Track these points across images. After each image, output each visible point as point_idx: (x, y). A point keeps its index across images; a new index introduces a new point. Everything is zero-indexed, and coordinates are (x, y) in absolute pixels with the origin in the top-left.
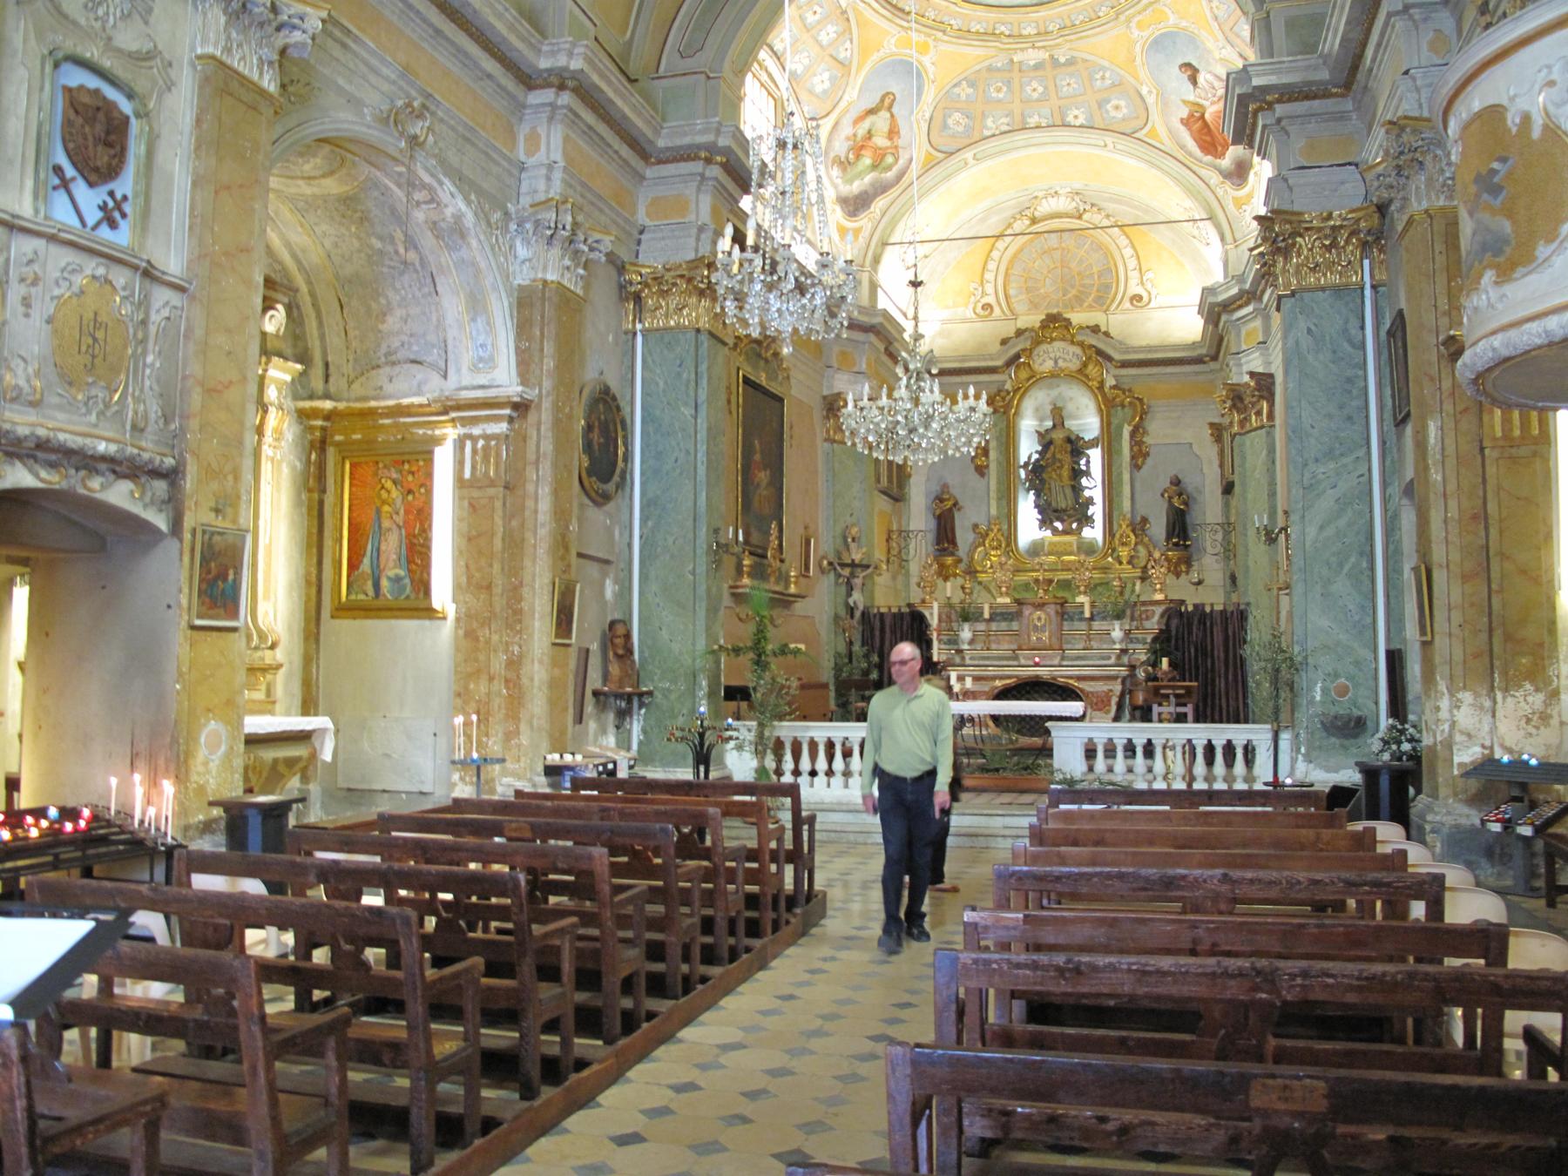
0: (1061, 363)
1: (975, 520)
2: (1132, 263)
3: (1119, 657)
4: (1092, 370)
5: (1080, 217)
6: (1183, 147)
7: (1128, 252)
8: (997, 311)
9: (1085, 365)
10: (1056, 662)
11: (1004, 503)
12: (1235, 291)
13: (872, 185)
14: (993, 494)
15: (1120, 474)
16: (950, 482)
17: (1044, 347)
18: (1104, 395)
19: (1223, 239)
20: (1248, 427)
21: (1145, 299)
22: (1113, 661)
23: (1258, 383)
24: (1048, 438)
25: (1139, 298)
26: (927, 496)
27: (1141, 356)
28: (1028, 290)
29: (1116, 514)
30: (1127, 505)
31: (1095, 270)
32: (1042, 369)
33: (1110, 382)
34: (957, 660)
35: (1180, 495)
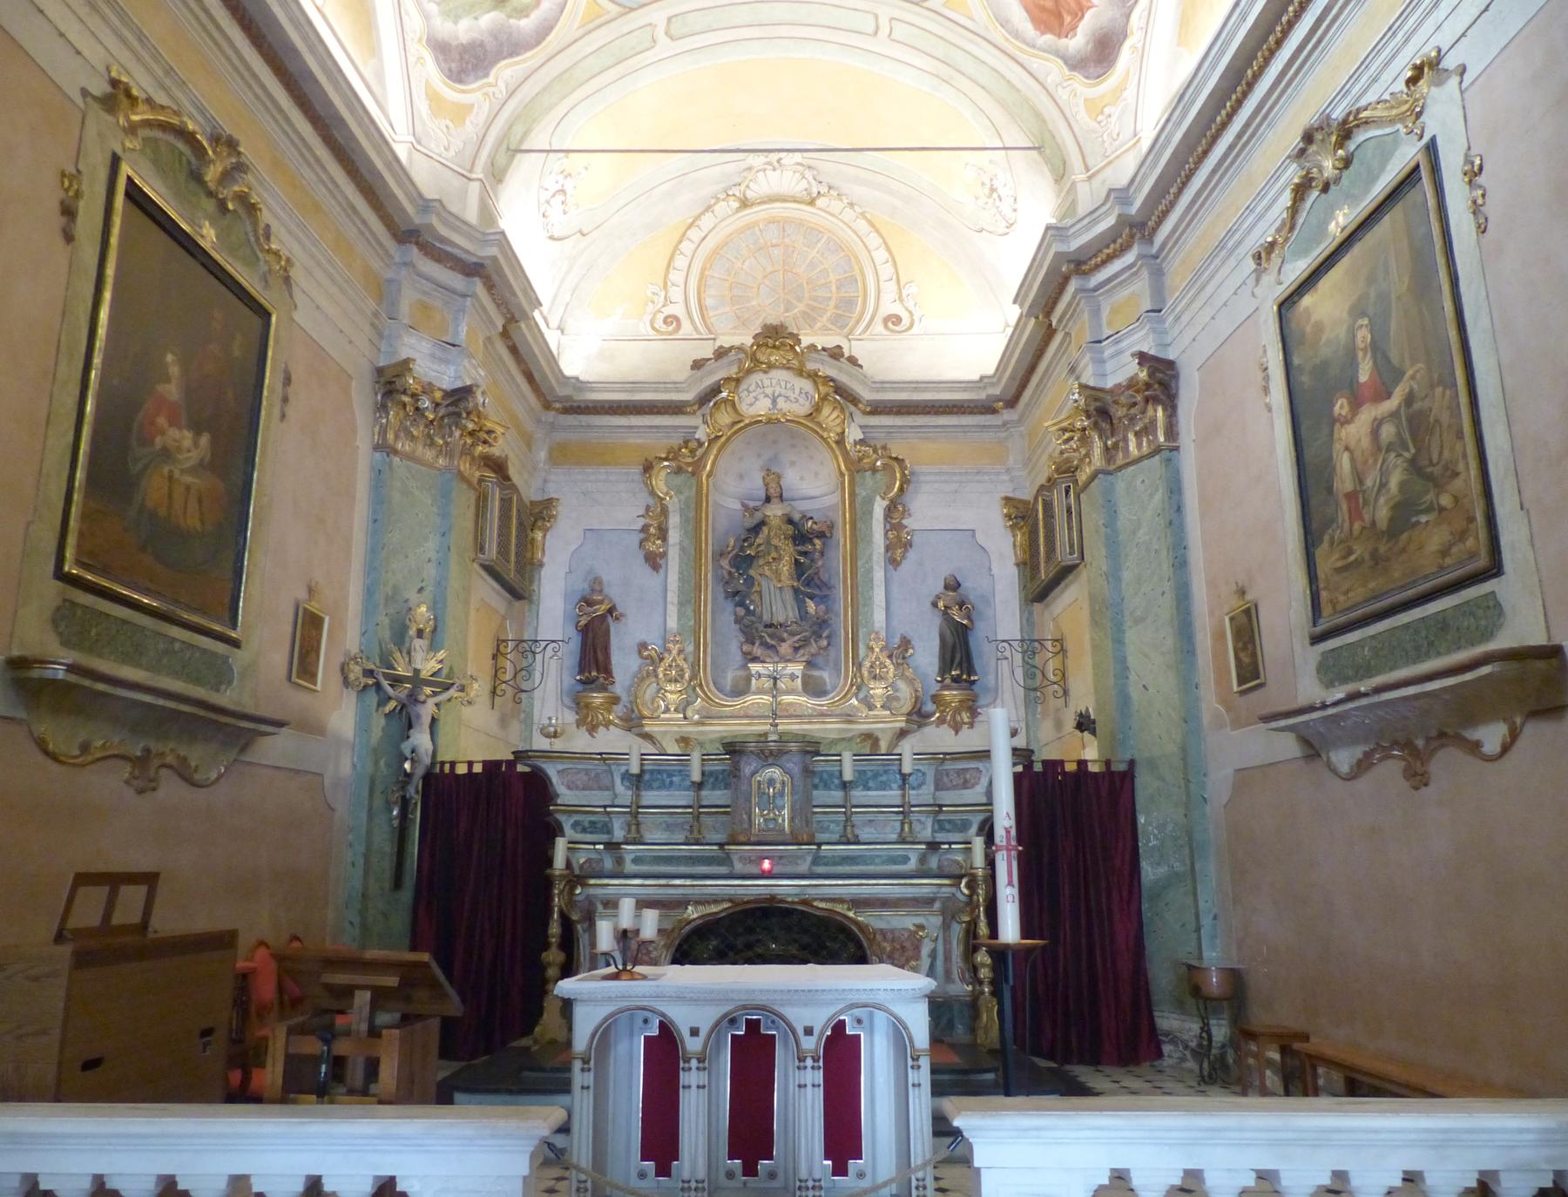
0: (781, 403)
1: (642, 636)
2: (886, 271)
3: (923, 859)
4: (829, 416)
5: (812, 203)
6: (1004, 23)
7: (881, 255)
8: (686, 328)
9: (817, 409)
10: (803, 867)
11: (689, 612)
12: (1109, 222)
13: (495, 34)
14: (672, 597)
15: (870, 570)
16: (605, 579)
17: (757, 377)
18: (845, 453)
19: (1060, 174)
20: (1120, 459)
21: (906, 321)
22: (912, 865)
23: (1150, 375)
24: (758, 516)
25: (897, 320)
26: (566, 596)
27: (903, 396)
29: (862, 632)
30: (879, 617)
31: (832, 277)
32: (752, 411)
33: (853, 434)
34: (608, 864)
35: (961, 604)
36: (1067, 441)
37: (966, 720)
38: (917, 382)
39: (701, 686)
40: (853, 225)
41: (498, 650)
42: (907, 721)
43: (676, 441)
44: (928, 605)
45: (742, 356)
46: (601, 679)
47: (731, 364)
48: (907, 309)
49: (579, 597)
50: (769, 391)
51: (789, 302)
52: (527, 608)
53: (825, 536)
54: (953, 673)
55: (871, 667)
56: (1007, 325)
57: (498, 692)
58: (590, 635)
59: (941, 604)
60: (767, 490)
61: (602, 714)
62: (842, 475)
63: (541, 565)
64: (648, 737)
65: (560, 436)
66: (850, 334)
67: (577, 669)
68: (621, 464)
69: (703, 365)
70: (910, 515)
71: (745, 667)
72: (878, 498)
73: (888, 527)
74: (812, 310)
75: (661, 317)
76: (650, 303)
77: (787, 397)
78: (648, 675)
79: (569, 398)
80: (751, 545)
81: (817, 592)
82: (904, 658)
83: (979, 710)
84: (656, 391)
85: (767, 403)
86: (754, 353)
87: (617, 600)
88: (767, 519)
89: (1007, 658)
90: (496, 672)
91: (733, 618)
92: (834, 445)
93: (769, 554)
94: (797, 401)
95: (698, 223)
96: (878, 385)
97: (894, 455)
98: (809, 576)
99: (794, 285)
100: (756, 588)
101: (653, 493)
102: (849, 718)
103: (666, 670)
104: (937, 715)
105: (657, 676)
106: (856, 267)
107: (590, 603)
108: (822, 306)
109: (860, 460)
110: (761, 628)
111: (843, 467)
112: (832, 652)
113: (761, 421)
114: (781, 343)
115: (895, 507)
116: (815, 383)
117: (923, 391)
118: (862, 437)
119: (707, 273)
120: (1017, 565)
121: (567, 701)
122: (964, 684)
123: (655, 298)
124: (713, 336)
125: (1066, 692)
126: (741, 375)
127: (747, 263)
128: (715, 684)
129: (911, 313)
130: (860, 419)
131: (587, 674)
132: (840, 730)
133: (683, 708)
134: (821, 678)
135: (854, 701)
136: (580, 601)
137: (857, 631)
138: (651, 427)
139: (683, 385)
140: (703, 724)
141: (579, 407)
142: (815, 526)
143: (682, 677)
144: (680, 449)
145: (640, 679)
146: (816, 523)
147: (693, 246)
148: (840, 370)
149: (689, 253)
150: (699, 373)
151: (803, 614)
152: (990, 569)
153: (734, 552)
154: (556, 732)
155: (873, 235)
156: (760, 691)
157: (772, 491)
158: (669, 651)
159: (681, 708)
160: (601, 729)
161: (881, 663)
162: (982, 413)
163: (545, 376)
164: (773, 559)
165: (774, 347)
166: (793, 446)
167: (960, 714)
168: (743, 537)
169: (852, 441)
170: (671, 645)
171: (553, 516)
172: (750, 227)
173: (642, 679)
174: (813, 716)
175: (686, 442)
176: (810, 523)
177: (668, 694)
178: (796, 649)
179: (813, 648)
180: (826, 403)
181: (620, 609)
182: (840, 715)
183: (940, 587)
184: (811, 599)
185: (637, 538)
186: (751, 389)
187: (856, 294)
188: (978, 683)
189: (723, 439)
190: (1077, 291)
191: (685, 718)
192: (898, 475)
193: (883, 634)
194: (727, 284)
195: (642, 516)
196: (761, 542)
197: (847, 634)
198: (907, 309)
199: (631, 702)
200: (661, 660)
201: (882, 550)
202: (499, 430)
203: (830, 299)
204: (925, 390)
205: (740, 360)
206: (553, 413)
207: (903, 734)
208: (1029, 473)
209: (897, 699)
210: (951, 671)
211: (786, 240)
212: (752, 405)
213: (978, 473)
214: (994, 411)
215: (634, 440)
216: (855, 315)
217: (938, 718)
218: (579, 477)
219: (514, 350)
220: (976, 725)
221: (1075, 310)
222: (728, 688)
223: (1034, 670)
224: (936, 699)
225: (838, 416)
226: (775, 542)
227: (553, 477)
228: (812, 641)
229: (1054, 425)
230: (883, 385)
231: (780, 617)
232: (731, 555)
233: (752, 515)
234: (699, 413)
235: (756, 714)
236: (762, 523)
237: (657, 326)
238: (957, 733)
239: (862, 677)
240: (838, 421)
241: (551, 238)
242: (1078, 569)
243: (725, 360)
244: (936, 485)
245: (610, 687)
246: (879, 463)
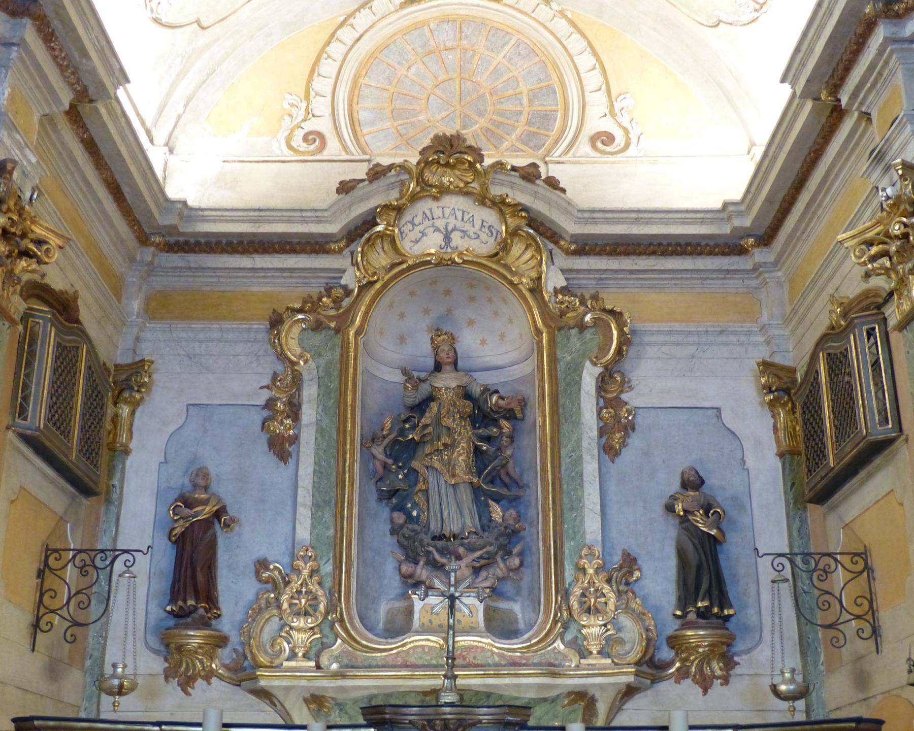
0: (457, 240)
1: (261, 551)
2: (593, 80)
7: (585, 61)
8: (333, 148)
9: (506, 246)
11: (328, 517)
14: (305, 496)
16: (213, 471)
18: (543, 305)
21: (620, 140)
24: (425, 389)
25: (609, 138)
28: (395, 114)
29: (568, 547)
31: (523, 88)
32: (418, 250)
33: (554, 280)
35: (707, 508)
36: (873, 259)
37: (718, 673)
38: (639, 211)
39: (341, 621)
40: (550, 25)
41: (46, 564)
42: (637, 674)
43: (315, 289)
44: (659, 510)
45: (405, 177)
46: (201, 611)
47: (391, 186)
48: (620, 126)
49: (176, 496)
50: (440, 224)
51: (466, 116)
52: (103, 509)
53: (516, 418)
54: (700, 604)
55: (583, 595)
56: (753, 144)
57: (42, 624)
58: (188, 548)
59: (679, 508)
60: (437, 354)
61: (201, 661)
62: (539, 332)
63: (127, 452)
64: (264, 694)
65: (160, 282)
66: (547, 155)
67: (169, 597)
68: (244, 319)
69: (353, 188)
70: (631, 388)
71: (405, 596)
72: (588, 364)
73: (602, 403)
74: (498, 127)
75: (300, 134)
76: (286, 117)
77: (463, 231)
78: (268, 604)
79: (172, 230)
80: (413, 428)
81: (504, 491)
82: (627, 584)
83: (736, 659)
84: (289, 221)
85: (438, 238)
86: (421, 174)
87: (228, 500)
88: (437, 393)
89: (787, 580)
90: (42, 595)
91: (388, 527)
92: (528, 295)
93: (439, 439)
94: (478, 237)
95: (352, 21)
96: (586, 215)
97: (608, 307)
98: (494, 469)
99: (475, 95)
100: (421, 486)
101: (281, 356)
102: (552, 669)
103: (292, 598)
104: (678, 665)
105: (279, 607)
106: (554, 76)
107: (189, 503)
108: (511, 122)
109: (563, 314)
110: (427, 539)
111: (539, 323)
112: (527, 576)
113: (429, 262)
114: (457, 159)
115: (611, 376)
116: (502, 214)
117: (647, 223)
118: (564, 284)
119: (361, 80)
120: (781, 455)
121: (154, 642)
122: (714, 621)
123: (294, 111)
124: (367, 157)
125: (876, 632)
126: (404, 201)
127: (413, 70)
128: (362, 619)
129: (626, 131)
130: (562, 260)
131: (180, 603)
132: (541, 687)
133: (315, 653)
134: (511, 611)
135: (559, 645)
136: (176, 500)
137: (562, 546)
138: (282, 270)
139: (326, 214)
140: (344, 676)
141: (187, 243)
142: (501, 402)
143: (315, 608)
144: (320, 299)
145: (256, 611)
146: (502, 398)
147: (344, 49)
148: (535, 195)
149: (340, 58)
150: (347, 199)
151: (485, 521)
152: (743, 462)
153: (392, 436)
154: (121, 686)
155: (576, 36)
156: (426, 630)
157: (443, 355)
158: (298, 571)
159: (312, 653)
160: (200, 683)
161: (597, 590)
162: (724, 254)
163: (139, 194)
164: (444, 444)
165: (447, 165)
166: (472, 299)
167: (709, 664)
168: (403, 417)
169: (550, 289)
170: (301, 563)
171: (142, 385)
172: (417, 26)
173: (260, 611)
174: (501, 665)
175: (328, 291)
176: (495, 398)
177: (294, 634)
178: (476, 571)
179: (500, 569)
180: (516, 240)
181: (232, 512)
182: (539, 665)
183: (675, 486)
184: (497, 501)
185: (257, 417)
186: (417, 221)
187: (554, 108)
188: (733, 619)
189: (378, 286)
190: (887, 41)
191: (318, 667)
192: (615, 333)
193: (598, 550)
194: (387, 95)
195: (268, 387)
196: (428, 421)
197: (547, 549)
198: (620, 126)
199: (242, 644)
200: (287, 583)
201: (595, 433)
202: (54, 241)
203: (520, 113)
204: (648, 222)
205: (402, 183)
206: (152, 249)
207: (630, 691)
208: (793, 332)
209: (621, 642)
210: (696, 602)
211: (465, 42)
212: (417, 242)
213: (722, 332)
214: (742, 251)
215: (259, 287)
216: (554, 133)
217: (678, 670)
218: (183, 335)
219: (91, 146)
220: (732, 679)
221: (880, 74)
222: (381, 625)
223: (827, 597)
224: (674, 642)
225: (532, 257)
226: (447, 422)
227: (148, 335)
228: (499, 559)
229: (853, 237)
230: (593, 215)
231: (453, 526)
232: (386, 441)
233: (416, 387)
234: (346, 252)
235: (420, 662)
236: (431, 398)
237: (293, 144)
238: (705, 691)
239: (569, 609)
240: (533, 263)
241: (156, 21)
242: (893, 447)
243: (382, 182)
244: (665, 349)
245: (213, 622)
246: (588, 318)
